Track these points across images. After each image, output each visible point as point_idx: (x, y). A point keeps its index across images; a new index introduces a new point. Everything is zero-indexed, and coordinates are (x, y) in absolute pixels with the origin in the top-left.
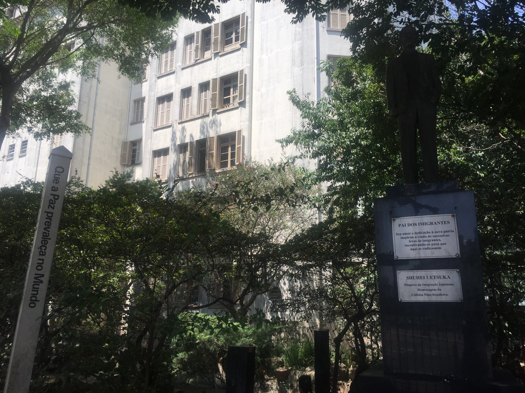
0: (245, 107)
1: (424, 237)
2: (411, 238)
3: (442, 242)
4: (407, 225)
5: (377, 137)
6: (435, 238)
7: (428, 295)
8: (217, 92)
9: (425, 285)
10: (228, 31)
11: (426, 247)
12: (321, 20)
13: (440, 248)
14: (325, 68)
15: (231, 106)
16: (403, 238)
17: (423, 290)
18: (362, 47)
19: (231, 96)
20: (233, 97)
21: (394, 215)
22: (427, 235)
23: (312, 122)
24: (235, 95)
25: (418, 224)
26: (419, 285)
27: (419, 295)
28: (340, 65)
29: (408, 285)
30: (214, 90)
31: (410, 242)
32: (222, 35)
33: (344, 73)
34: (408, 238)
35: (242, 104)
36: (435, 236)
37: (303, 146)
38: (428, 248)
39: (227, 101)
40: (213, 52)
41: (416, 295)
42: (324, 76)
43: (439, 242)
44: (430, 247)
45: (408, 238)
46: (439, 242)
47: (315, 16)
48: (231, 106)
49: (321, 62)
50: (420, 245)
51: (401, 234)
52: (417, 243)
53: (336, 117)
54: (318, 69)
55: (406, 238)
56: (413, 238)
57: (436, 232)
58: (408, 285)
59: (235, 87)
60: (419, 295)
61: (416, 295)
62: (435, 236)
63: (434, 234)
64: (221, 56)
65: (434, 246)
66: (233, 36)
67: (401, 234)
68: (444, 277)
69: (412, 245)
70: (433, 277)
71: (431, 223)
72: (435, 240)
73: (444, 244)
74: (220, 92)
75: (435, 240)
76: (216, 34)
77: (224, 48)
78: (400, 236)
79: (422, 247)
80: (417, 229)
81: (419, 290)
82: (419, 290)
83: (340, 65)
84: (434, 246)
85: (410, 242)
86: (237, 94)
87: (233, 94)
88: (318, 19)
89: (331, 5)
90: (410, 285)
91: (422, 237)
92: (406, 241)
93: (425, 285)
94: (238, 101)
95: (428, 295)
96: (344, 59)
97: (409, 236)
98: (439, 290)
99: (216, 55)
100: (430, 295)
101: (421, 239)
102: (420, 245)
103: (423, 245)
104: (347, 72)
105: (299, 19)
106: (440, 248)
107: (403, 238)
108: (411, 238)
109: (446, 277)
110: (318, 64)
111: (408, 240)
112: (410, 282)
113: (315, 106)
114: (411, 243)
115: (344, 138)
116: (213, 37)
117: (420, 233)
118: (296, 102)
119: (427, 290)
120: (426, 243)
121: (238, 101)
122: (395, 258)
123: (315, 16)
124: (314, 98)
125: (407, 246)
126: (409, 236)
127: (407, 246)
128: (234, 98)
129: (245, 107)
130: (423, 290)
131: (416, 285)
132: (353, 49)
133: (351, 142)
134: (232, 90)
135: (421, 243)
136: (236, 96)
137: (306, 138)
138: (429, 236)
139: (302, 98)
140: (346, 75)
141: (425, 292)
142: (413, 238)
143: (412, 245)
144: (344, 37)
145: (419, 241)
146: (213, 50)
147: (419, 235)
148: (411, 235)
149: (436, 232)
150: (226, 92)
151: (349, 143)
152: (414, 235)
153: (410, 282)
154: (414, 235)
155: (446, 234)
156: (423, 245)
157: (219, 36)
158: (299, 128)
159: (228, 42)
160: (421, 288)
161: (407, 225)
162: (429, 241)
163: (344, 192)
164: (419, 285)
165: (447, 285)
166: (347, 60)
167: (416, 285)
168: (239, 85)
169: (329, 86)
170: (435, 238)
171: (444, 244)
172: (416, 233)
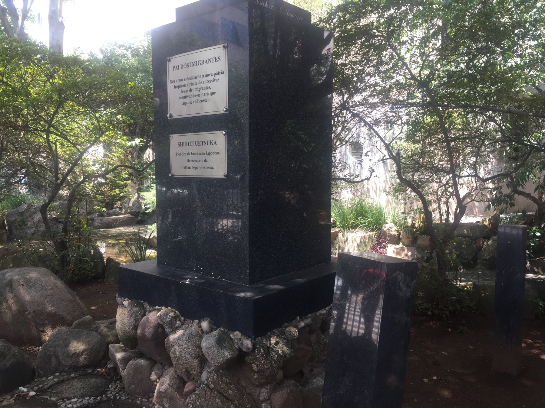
11: (196, 99)
13: (209, 100)
16: (176, 87)
22: (197, 81)
41: (186, 168)
43: (209, 91)
44: (200, 98)
61: (185, 168)
68: (211, 143)
69: (184, 97)
70: (201, 143)
81: (188, 161)
82: (188, 161)
84: (204, 98)
85: (182, 92)
90: (181, 154)
91: (193, 84)
95: (196, 168)
101: (192, 87)
103: (194, 96)
106: (209, 100)
107: (176, 87)
109: (213, 142)
112: (181, 150)
114: (184, 95)
120: (197, 93)
125: (179, 98)
127: (179, 98)
130: (192, 161)
143: (184, 97)
145: (191, 91)
149: (207, 76)
156: (194, 96)
160: (191, 158)
162: (199, 90)
172: (188, 79)
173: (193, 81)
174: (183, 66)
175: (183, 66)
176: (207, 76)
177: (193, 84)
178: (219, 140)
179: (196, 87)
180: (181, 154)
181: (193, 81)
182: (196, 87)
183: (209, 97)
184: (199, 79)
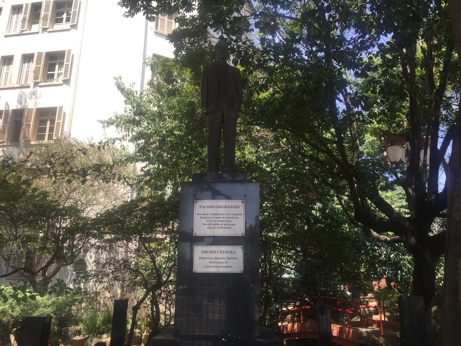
0: (69, 85)
1: (219, 218)
2: (208, 218)
3: (233, 223)
4: (206, 207)
5: (189, 131)
6: (227, 219)
7: (217, 267)
8: (41, 66)
9: (216, 258)
10: (60, 10)
11: (220, 226)
12: (150, 20)
13: (230, 228)
14: (150, 63)
15: (54, 82)
16: (201, 218)
17: (214, 263)
18: (184, 53)
19: (56, 72)
20: (58, 74)
21: (196, 198)
23: (134, 109)
24: (60, 72)
25: (215, 207)
26: (211, 258)
27: (210, 267)
28: (164, 64)
29: (202, 258)
30: (38, 62)
31: (207, 221)
32: (52, 13)
33: (167, 71)
34: (206, 218)
35: (66, 82)
36: (228, 218)
37: (123, 130)
38: (221, 228)
39: (51, 77)
40: (41, 26)
41: (208, 267)
42: (148, 70)
43: (230, 223)
44: (223, 226)
45: (206, 218)
46: (230, 223)
47: (146, 15)
48: (54, 82)
49: (147, 57)
50: (215, 224)
51: (200, 214)
52: (213, 223)
53: (156, 109)
54: (144, 63)
55: (204, 218)
56: (210, 218)
57: (228, 214)
58: (202, 258)
59: (61, 64)
60: (210, 267)
61: (208, 267)
62: (228, 218)
63: (227, 216)
64: (49, 32)
65: (226, 226)
66: (65, 16)
67: (200, 214)
68: (231, 252)
69: (209, 224)
70: (223, 252)
71: (226, 207)
72: (227, 221)
73: (234, 225)
74: (44, 66)
75: (227, 221)
76: (47, 10)
77: (53, 25)
78: (200, 216)
79: (216, 226)
80: (214, 211)
81: (210, 262)
82: (210, 262)
83: (164, 64)
84: (226, 226)
85: (207, 221)
86: (63, 71)
87: (58, 70)
88: (147, 18)
89: (160, 9)
90: (204, 258)
91: (217, 218)
92: (204, 221)
93: (216, 258)
94: (62, 78)
95: (217, 267)
96: (167, 60)
97: (207, 216)
98: (226, 262)
99: (44, 30)
100: (219, 267)
102: (215, 224)
103: (217, 224)
104: (169, 71)
105: (131, 14)
106: (230, 228)
108: (208, 218)
110: (144, 59)
111: (206, 219)
112: (204, 255)
113: (138, 95)
115: (161, 128)
116: (43, 13)
117: (216, 214)
118: (122, 89)
119: (217, 263)
120: (220, 223)
121: (62, 78)
122: (194, 235)
123: (146, 15)
124: (137, 88)
126: (207, 216)
128: (59, 75)
129: (69, 85)
130: (214, 263)
131: (208, 258)
132: (176, 53)
133: (167, 131)
134: (57, 66)
135: (216, 223)
136: (61, 73)
137: (127, 123)
138: (223, 218)
139: (127, 86)
140: (168, 73)
141: (215, 264)
142: (210, 218)
143: (209, 224)
144: (169, 41)
145: (215, 221)
146: (41, 24)
147: (215, 216)
148: (209, 216)
149: (228, 214)
150: (51, 67)
151: (165, 133)
152: (211, 216)
153: (204, 255)
154: (211, 216)
155: (236, 216)
156: (217, 224)
157: (50, 13)
158: (121, 112)
159: (59, 21)
161: (206, 207)
163: (158, 175)
164: (211, 258)
165: (233, 258)
166: (170, 60)
167: (208, 258)
168: (65, 63)
169: (152, 80)
170: (227, 219)
171: (234, 225)
172: (213, 214)
173: (218, 216)
174: (209, 207)
175: (209, 207)
176: (230, 214)
177: (217, 218)
178: (239, 251)
179: (220, 219)
180: (204, 258)
181: (218, 216)
182: (220, 219)
183: (230, 226)
184: (223, 216)
